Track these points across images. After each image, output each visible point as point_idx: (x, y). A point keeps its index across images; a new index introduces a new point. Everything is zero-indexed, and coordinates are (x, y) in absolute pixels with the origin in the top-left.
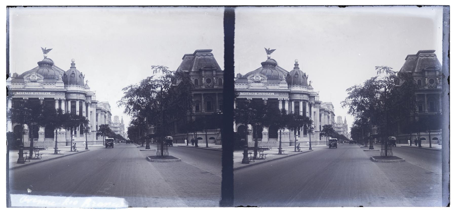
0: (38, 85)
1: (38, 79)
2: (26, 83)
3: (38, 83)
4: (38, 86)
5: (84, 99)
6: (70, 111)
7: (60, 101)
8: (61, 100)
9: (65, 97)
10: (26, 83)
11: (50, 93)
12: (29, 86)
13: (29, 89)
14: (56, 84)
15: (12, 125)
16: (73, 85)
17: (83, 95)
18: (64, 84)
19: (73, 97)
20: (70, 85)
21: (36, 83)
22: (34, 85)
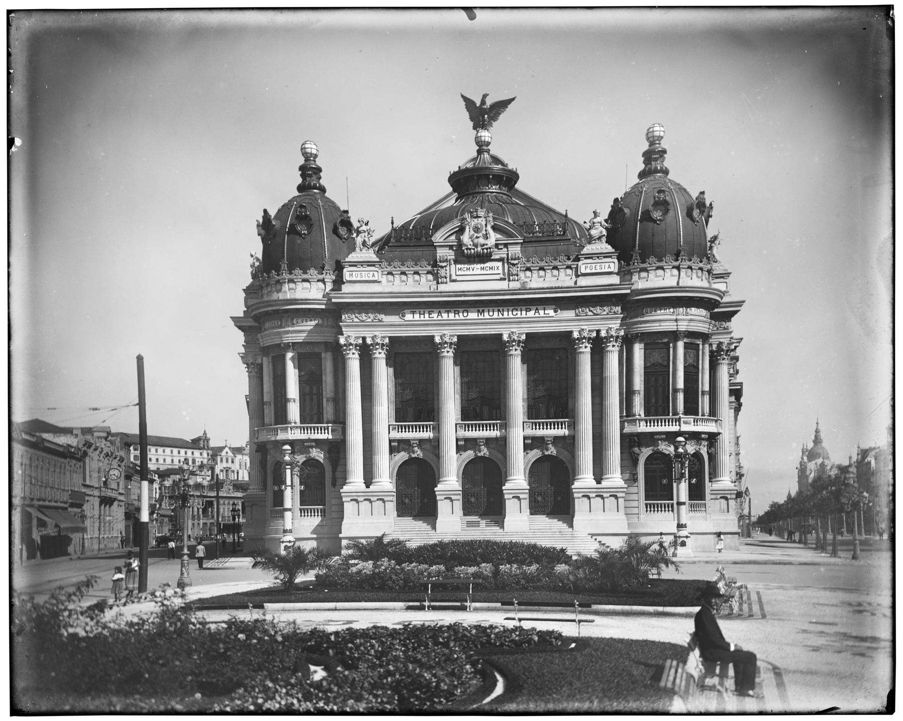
0: (500, 271)
1: (497, 246)
2: (443, 264)
3: (500, 264)
4: (498, 277)
5: (705, 331)
6: (643, 389)
7: (599, 345)
8: (602, 338)
9: (621, 325)
10: (442, 267)
11: (554, 306)
12: (459, 278)
13: (463, 293)
14: (580, 263)
15: (391, 459)
16: (659, 264)
17: (699, 313)
18: (616, 261)
19: (660, 321)
20: (643, 262)
21: (489, 264)
22: (479, 272)
